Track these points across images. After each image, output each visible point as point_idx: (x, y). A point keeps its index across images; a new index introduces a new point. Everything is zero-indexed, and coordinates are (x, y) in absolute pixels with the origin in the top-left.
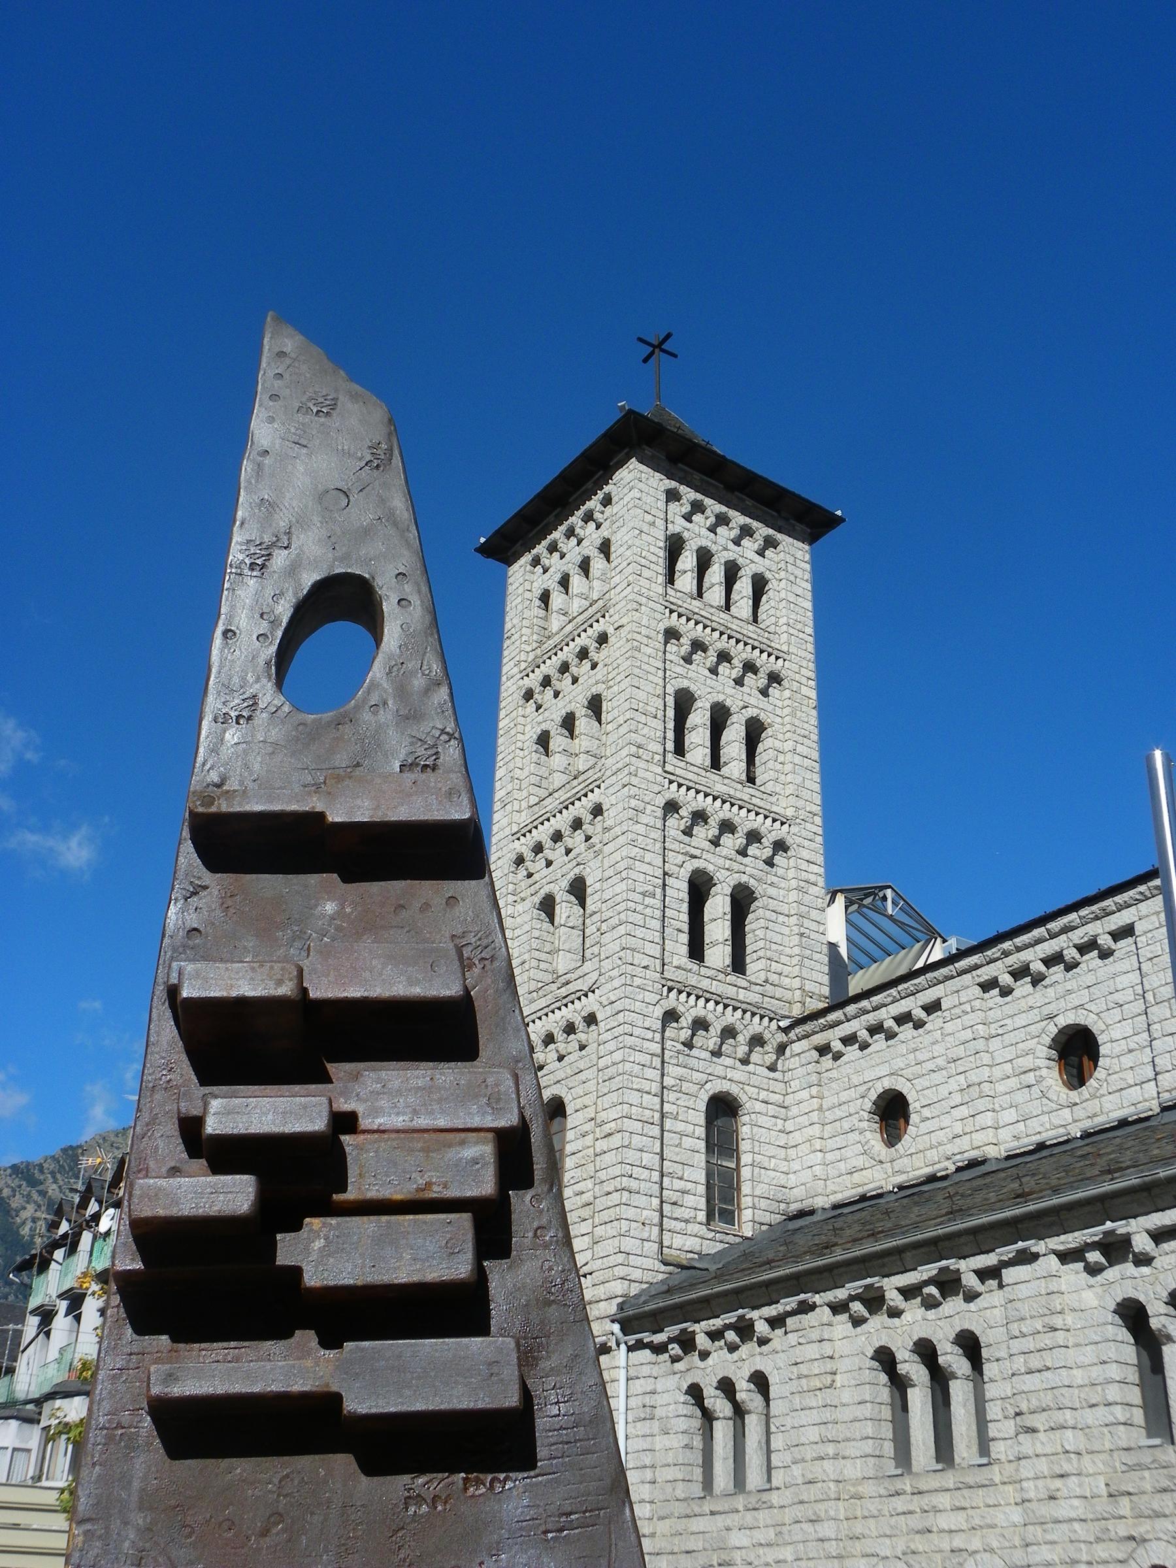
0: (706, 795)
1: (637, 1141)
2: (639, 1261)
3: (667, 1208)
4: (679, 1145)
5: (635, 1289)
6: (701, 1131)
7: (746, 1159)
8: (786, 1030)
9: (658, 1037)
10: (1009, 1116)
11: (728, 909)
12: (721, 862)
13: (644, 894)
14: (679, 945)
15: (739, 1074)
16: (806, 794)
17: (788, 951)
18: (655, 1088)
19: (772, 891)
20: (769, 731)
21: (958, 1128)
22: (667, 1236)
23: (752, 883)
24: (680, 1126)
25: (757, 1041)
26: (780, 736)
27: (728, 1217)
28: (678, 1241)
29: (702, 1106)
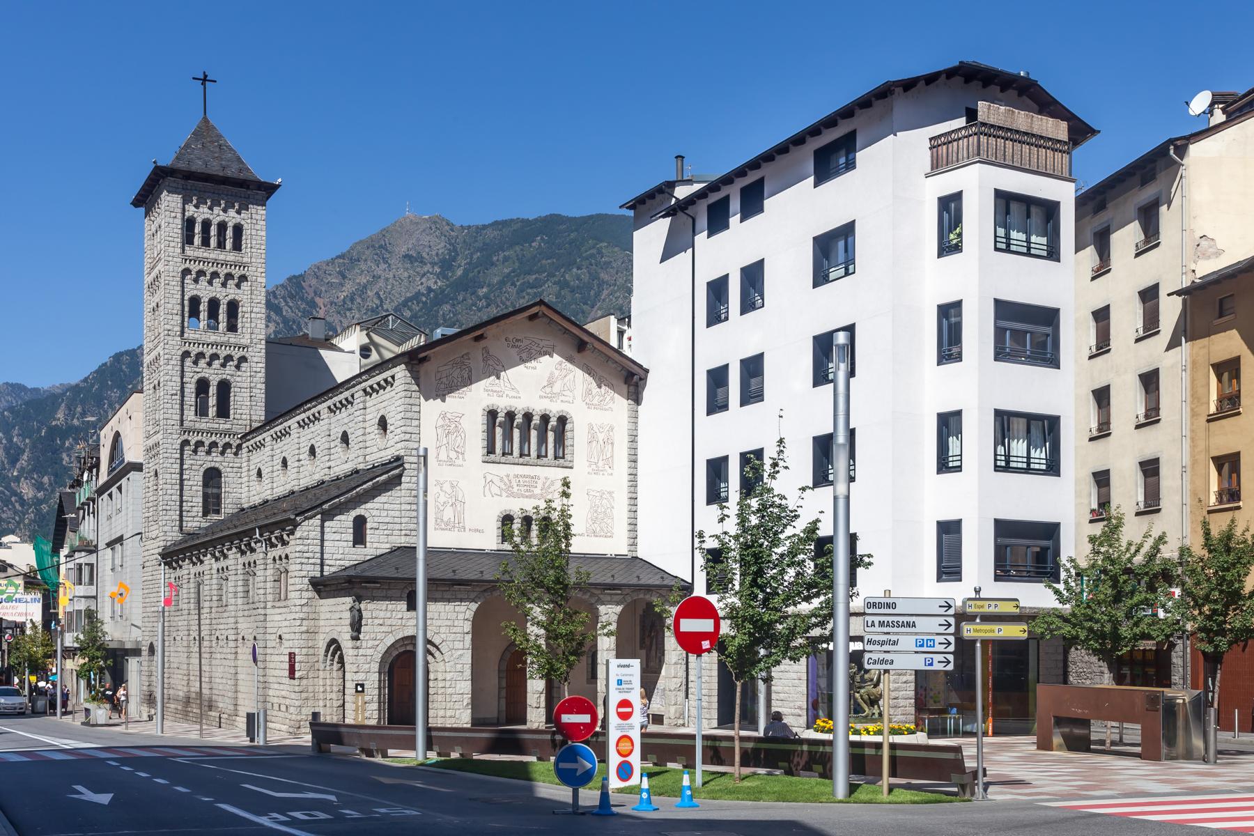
0: (204, 344)
1: (169, 492)
2: (171, 534)
3: (184, 513)
4: (191, 490)
5: (169, 544)
6: (200, 483)
7: (223, 490)
8: (241, 438)
9: (178, 451)
10: (275, 486)
11: (215, 392)
12: (212, 371)
13: (172, 395)
14: (190, 414)
15: (220, 458)
16: (256, 331)
17: (246, 403)
18: (178, 471)
19: (238, 379)
20: (240, 304)
21: (265, 488)
22: (184, 524)
23: (229, 377)
24: (191, 483)
25: (227, 446)
26: (246, 305)
27: (218, 512)
28: (189, 525)
29: (201, 474)
